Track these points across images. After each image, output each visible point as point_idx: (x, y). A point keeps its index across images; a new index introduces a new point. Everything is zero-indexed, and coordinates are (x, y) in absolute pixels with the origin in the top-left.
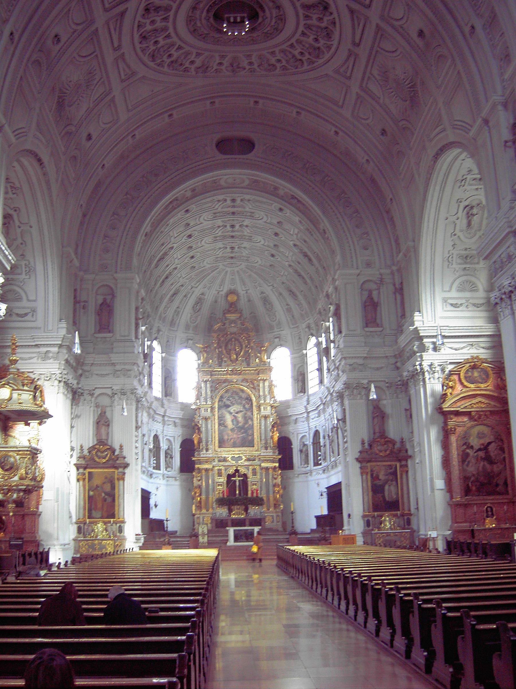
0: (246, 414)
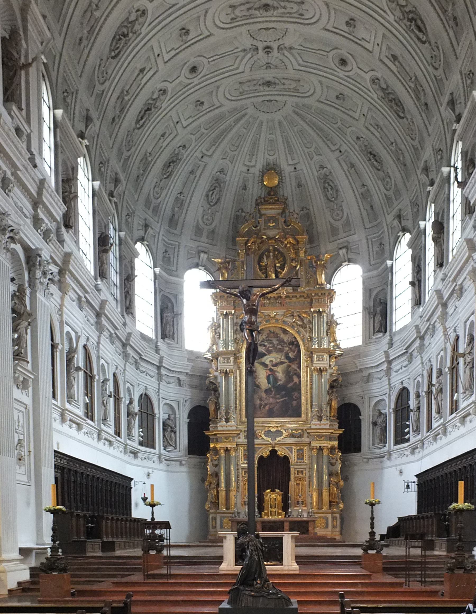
0: (289, 366)
